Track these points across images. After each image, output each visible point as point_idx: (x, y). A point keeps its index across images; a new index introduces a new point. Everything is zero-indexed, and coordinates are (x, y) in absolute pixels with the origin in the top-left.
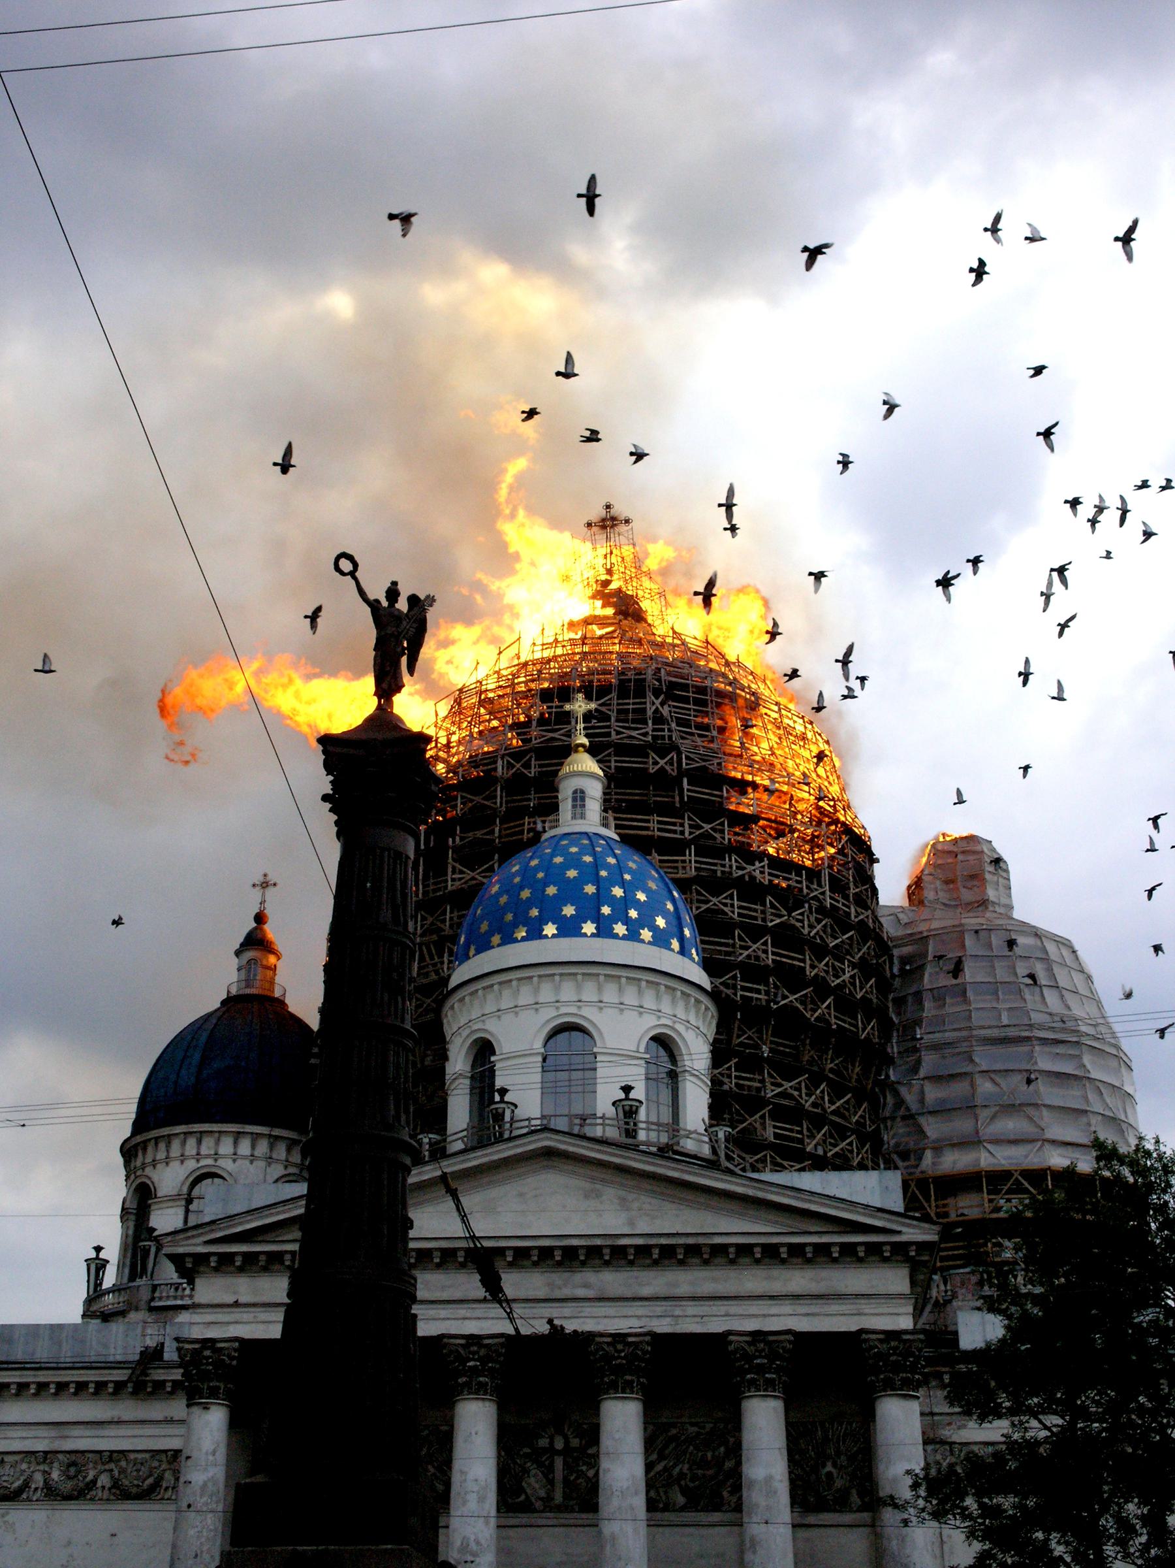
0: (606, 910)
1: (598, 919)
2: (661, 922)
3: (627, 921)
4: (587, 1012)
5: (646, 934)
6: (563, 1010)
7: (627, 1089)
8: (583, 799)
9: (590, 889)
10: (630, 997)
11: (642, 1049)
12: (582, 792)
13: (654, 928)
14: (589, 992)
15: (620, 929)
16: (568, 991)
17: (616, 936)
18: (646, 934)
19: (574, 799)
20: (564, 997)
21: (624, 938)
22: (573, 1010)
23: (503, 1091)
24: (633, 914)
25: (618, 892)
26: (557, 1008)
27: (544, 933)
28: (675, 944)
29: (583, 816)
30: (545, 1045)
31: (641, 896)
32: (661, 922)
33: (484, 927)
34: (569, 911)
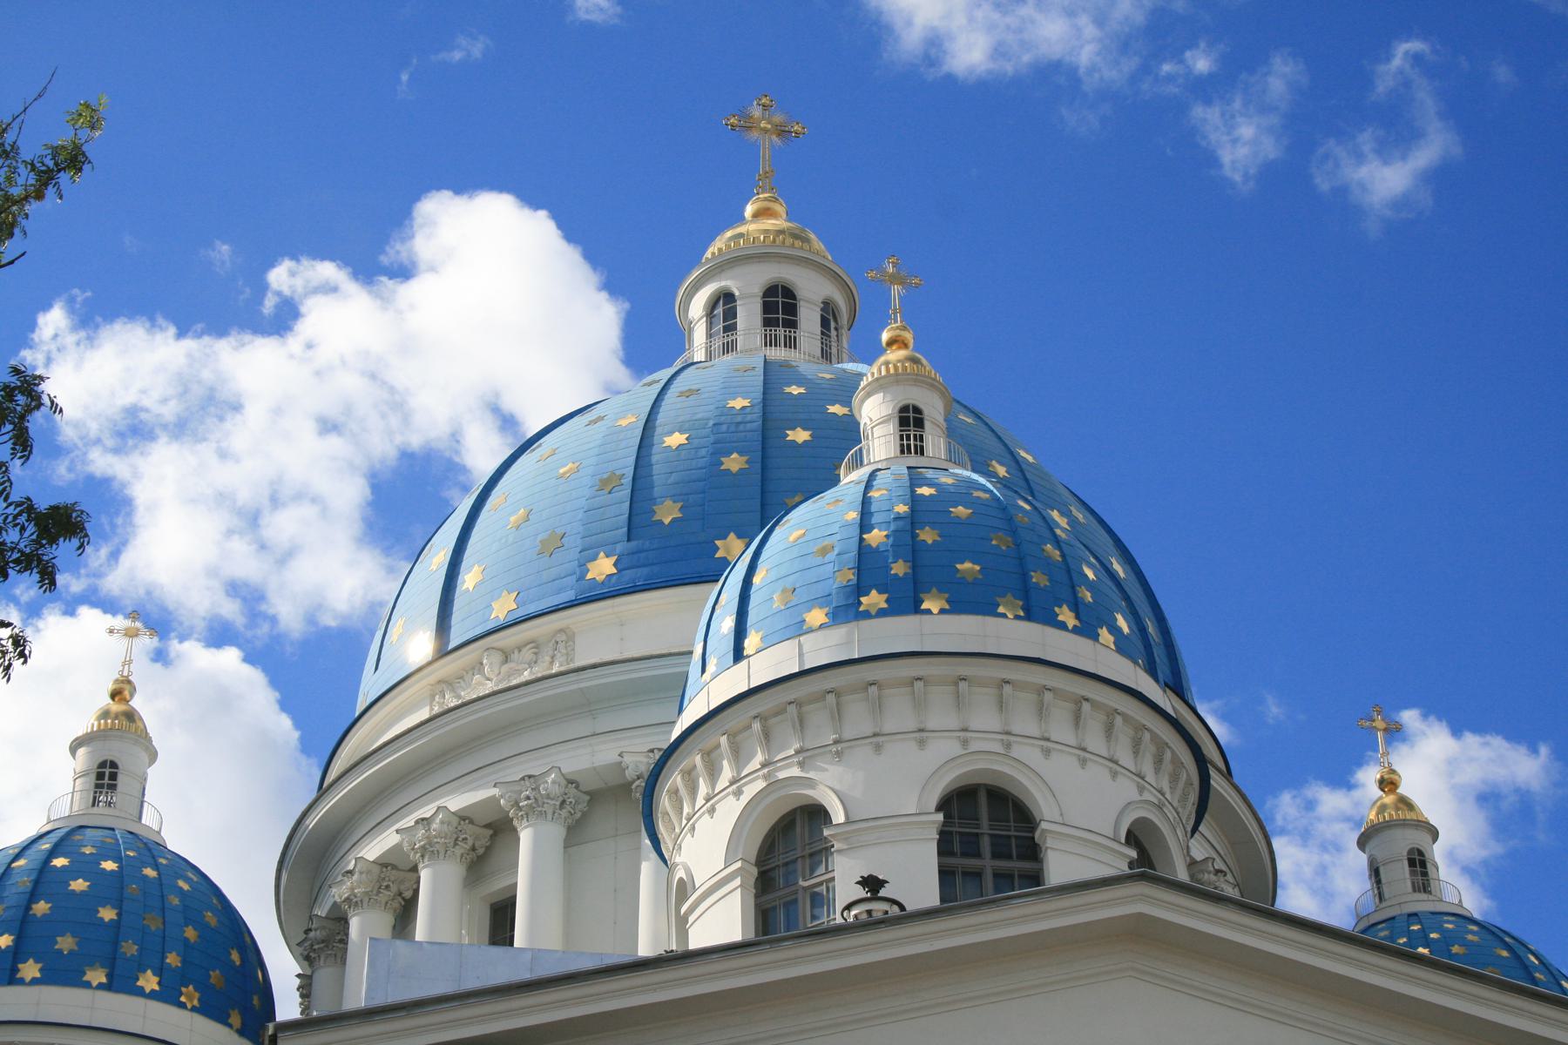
0: (1038, 578)
3: (1076, 606)
4: (1029, 753)
5: (1105, 636)
6: (974, 747)
8: (919, 423)
11: (1123, 841)
12: (917, 410)
17: (1062, 626)
19: (904, 422)
20: (976, 723)
21: (1075, 631)
22: (998, 748)
26: (965, 743)
27: (924, 606)
29: (920, 451)
30: (939, 809)
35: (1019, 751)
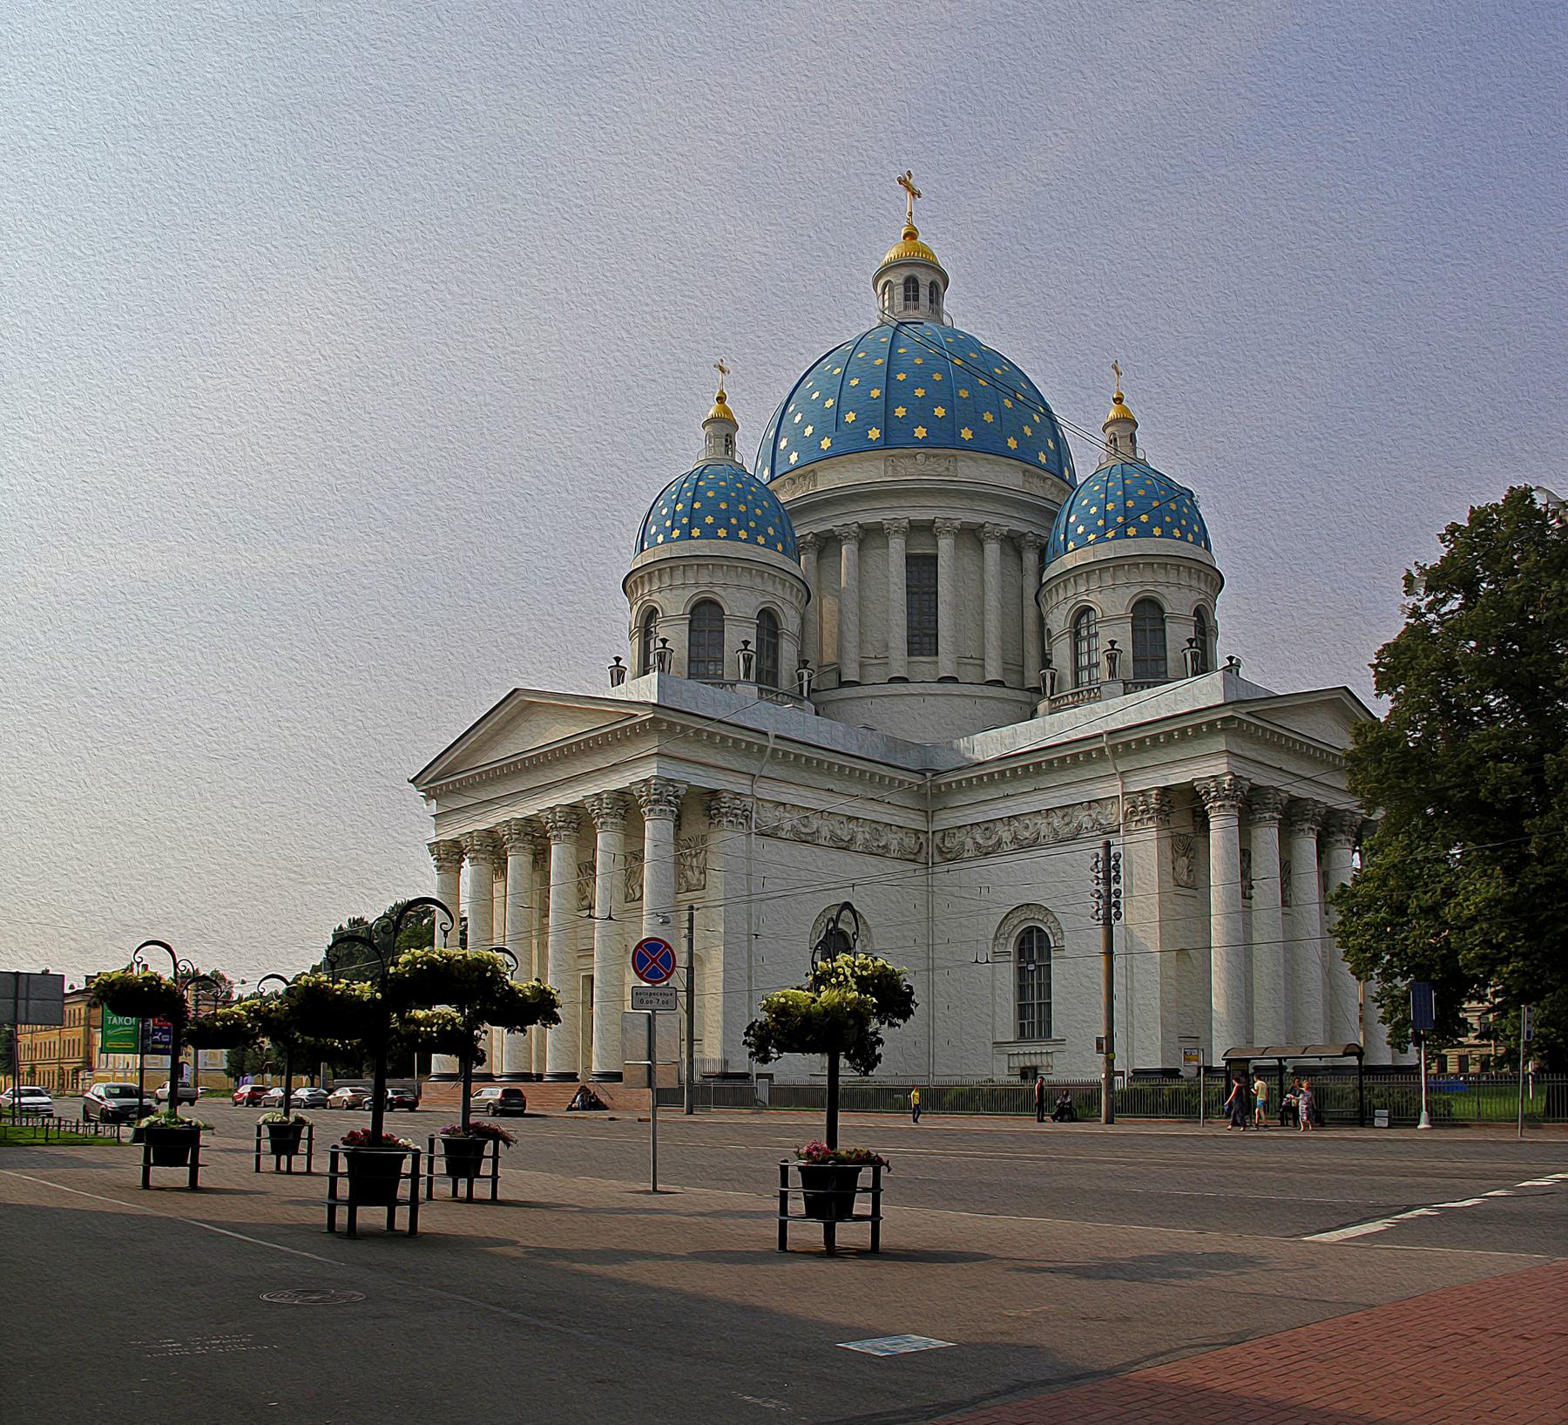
0: (734, 521)
1: (728, 527)
2: (771, 531)
7: (746, 643)
9: (723, 506)
10: (745, 581)
13: (766, 534)
14: (719, 578)
15: (743, 534)
16: (704, 578)
18: (761, 540)
23: (664, 641)
24: (752, 524)
25: (742, 508)
28: (780, 547)
31: (758, 512)
32: (771, 531)
33: (653, 530)
34: (709, 520)
35: (715, 589)
